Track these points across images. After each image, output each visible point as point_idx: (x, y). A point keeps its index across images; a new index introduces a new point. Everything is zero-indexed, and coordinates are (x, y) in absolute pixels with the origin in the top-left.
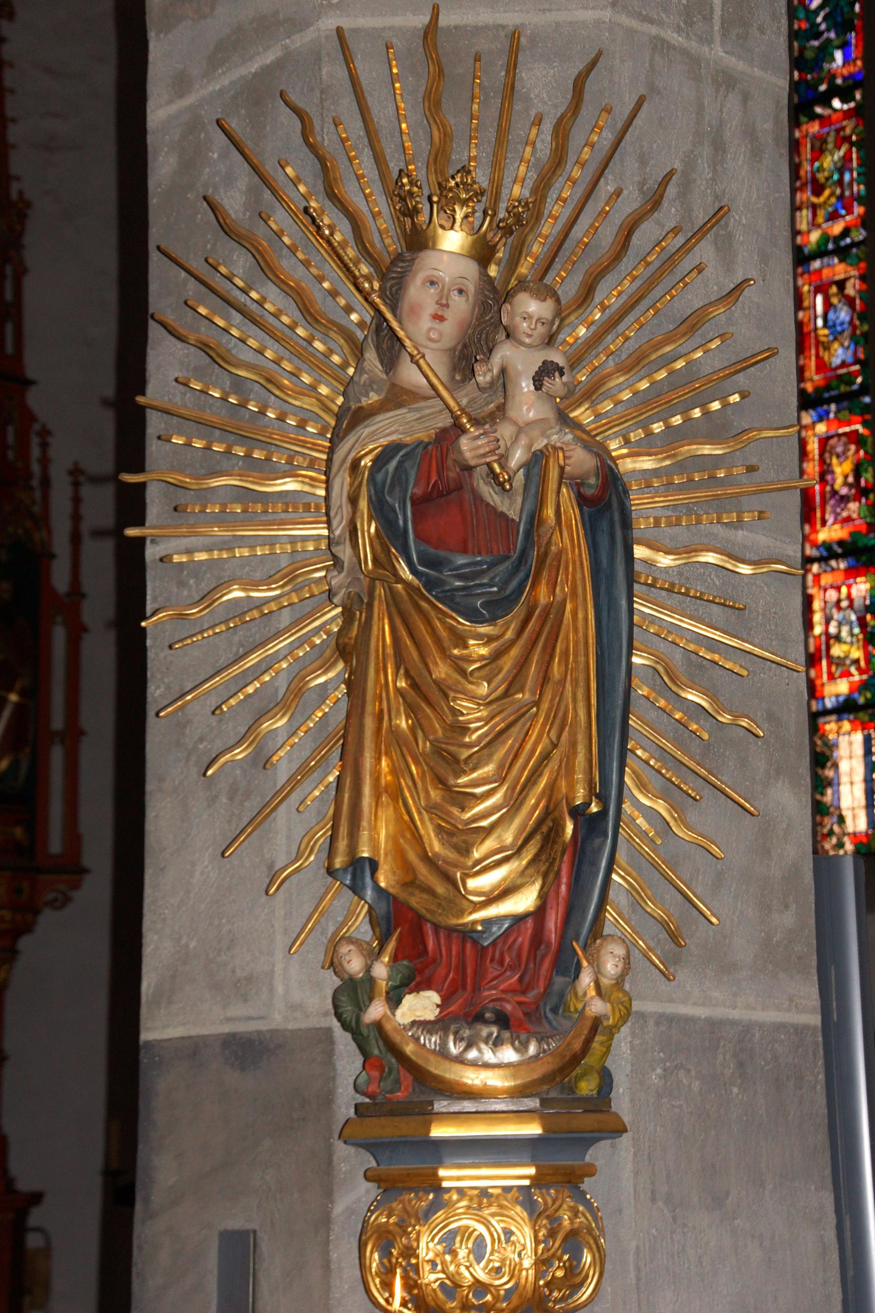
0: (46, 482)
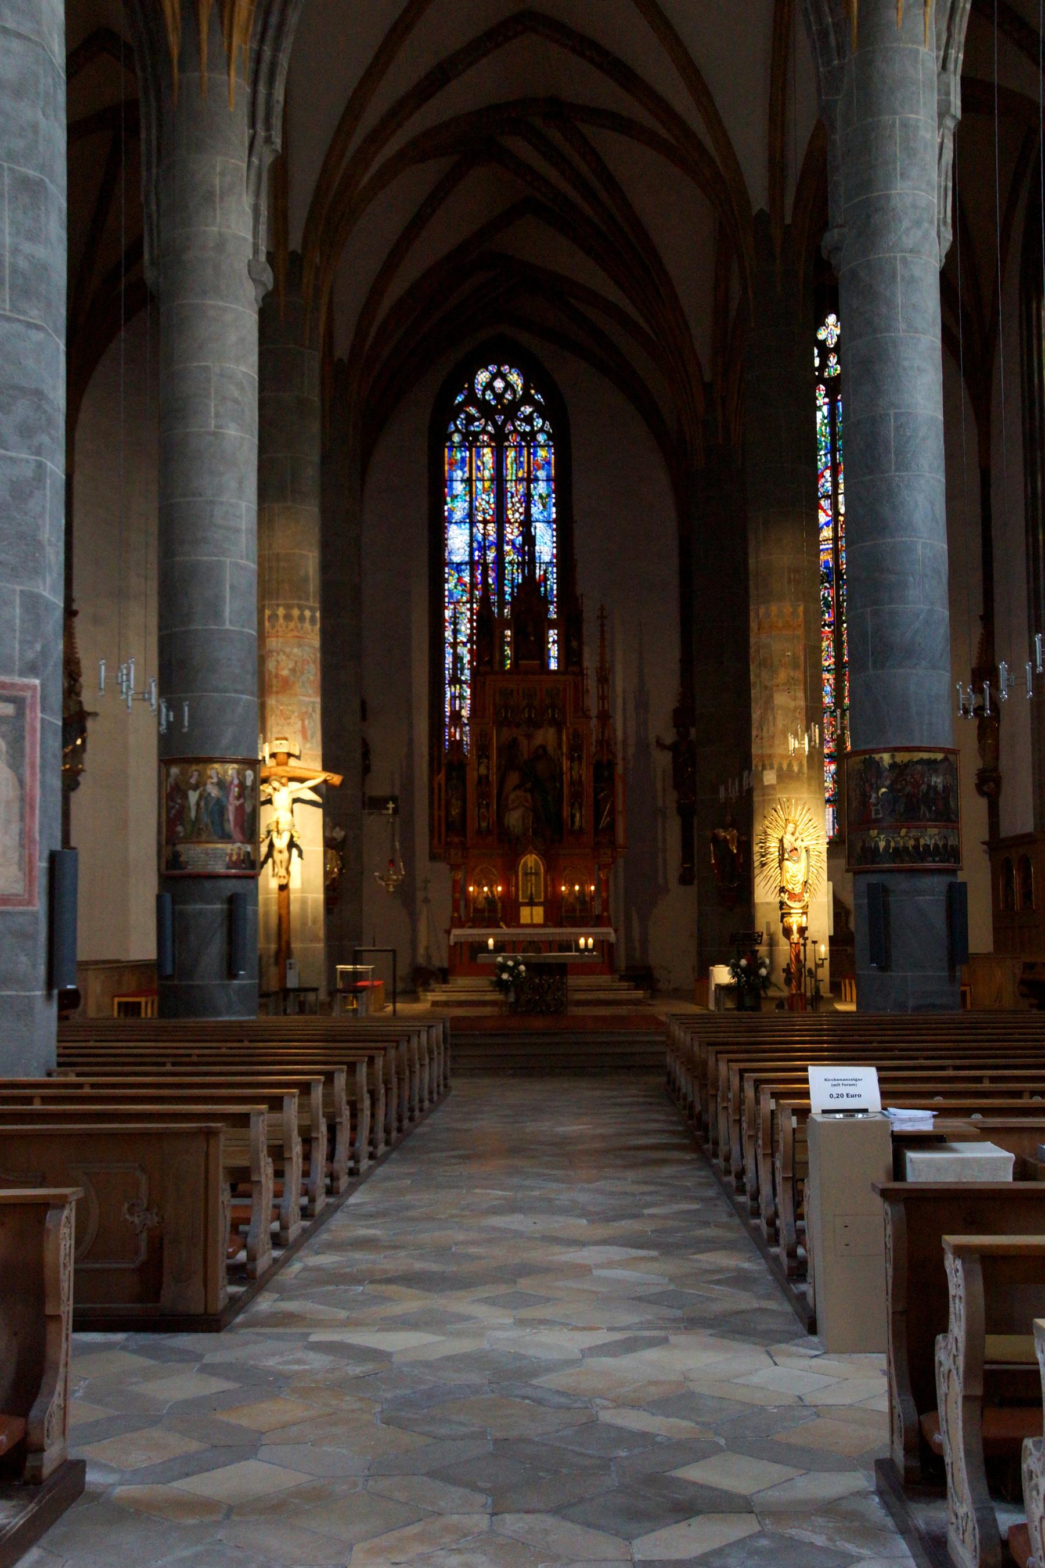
0: (615, 743)
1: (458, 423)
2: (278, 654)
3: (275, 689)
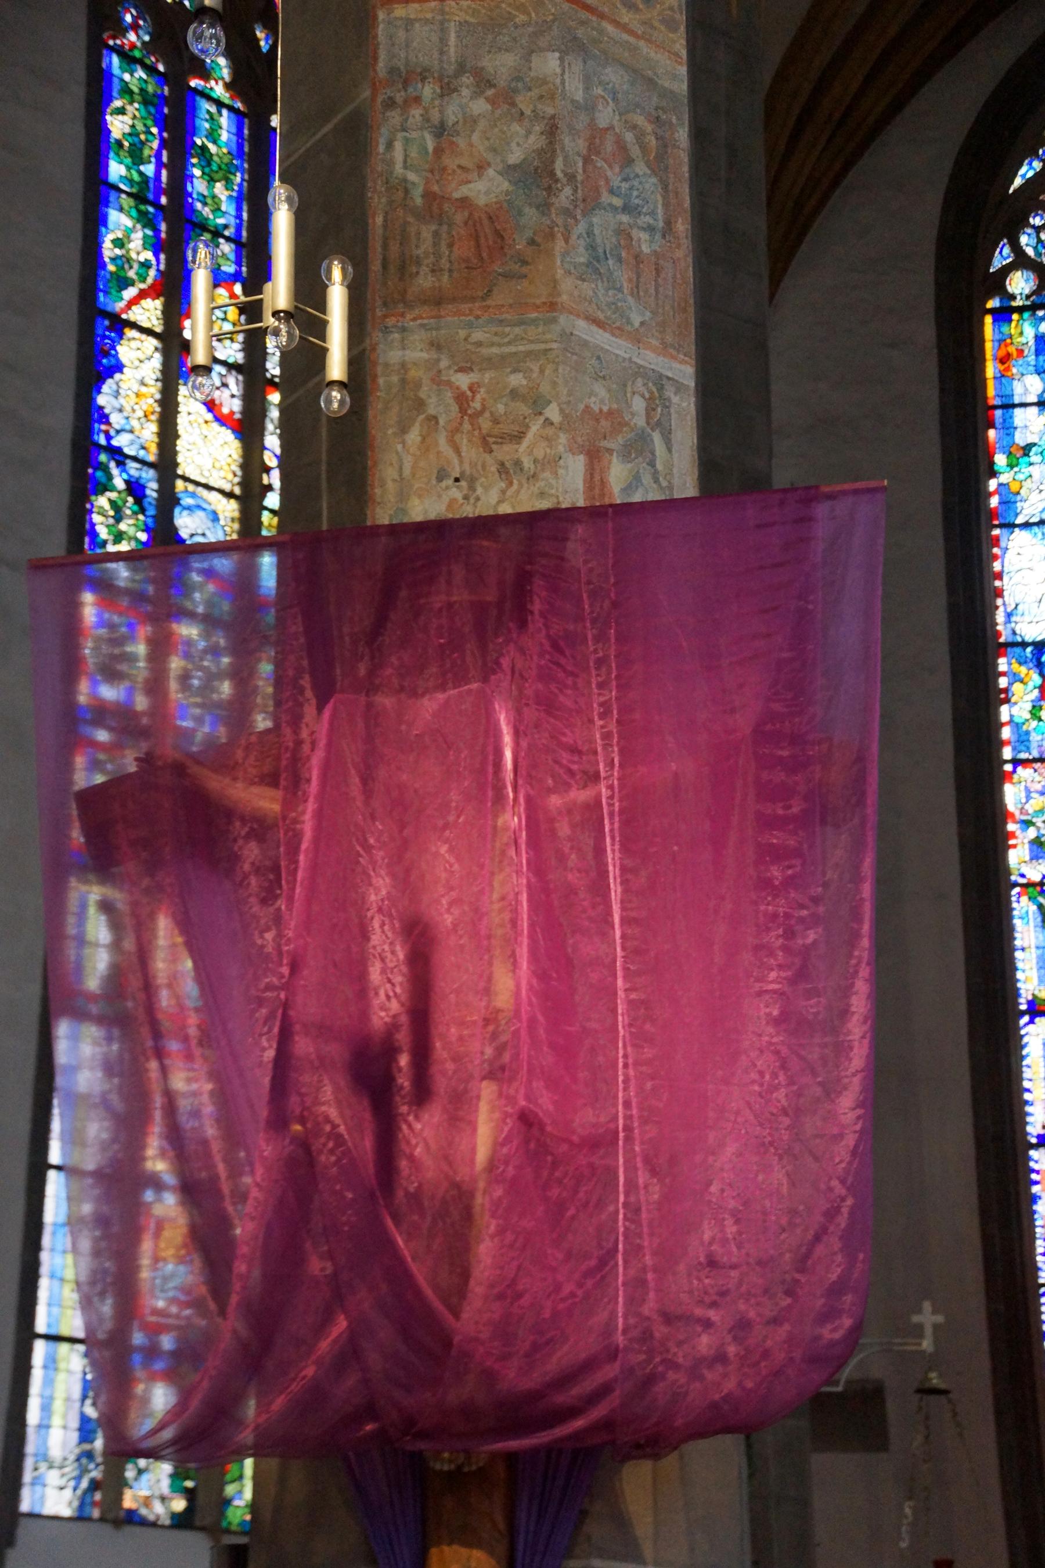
1: (1024, 240)
2: (448, 89)
3: (425, 281)
